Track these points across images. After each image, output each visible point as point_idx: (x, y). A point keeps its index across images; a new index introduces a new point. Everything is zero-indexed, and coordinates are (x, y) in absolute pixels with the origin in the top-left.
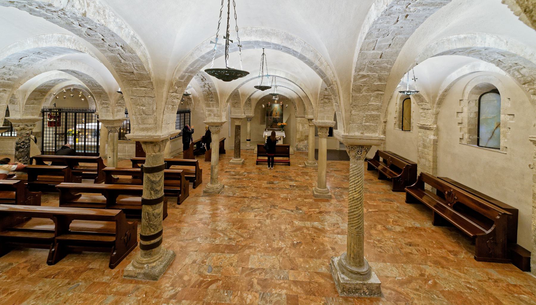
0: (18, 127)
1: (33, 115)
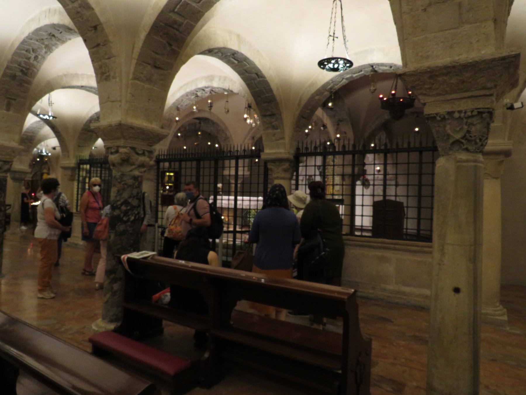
0: (117, 155)
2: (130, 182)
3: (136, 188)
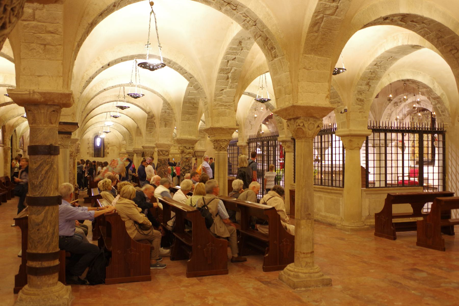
1: (190, 135)
2: (185, 160)
3: (187, 162)
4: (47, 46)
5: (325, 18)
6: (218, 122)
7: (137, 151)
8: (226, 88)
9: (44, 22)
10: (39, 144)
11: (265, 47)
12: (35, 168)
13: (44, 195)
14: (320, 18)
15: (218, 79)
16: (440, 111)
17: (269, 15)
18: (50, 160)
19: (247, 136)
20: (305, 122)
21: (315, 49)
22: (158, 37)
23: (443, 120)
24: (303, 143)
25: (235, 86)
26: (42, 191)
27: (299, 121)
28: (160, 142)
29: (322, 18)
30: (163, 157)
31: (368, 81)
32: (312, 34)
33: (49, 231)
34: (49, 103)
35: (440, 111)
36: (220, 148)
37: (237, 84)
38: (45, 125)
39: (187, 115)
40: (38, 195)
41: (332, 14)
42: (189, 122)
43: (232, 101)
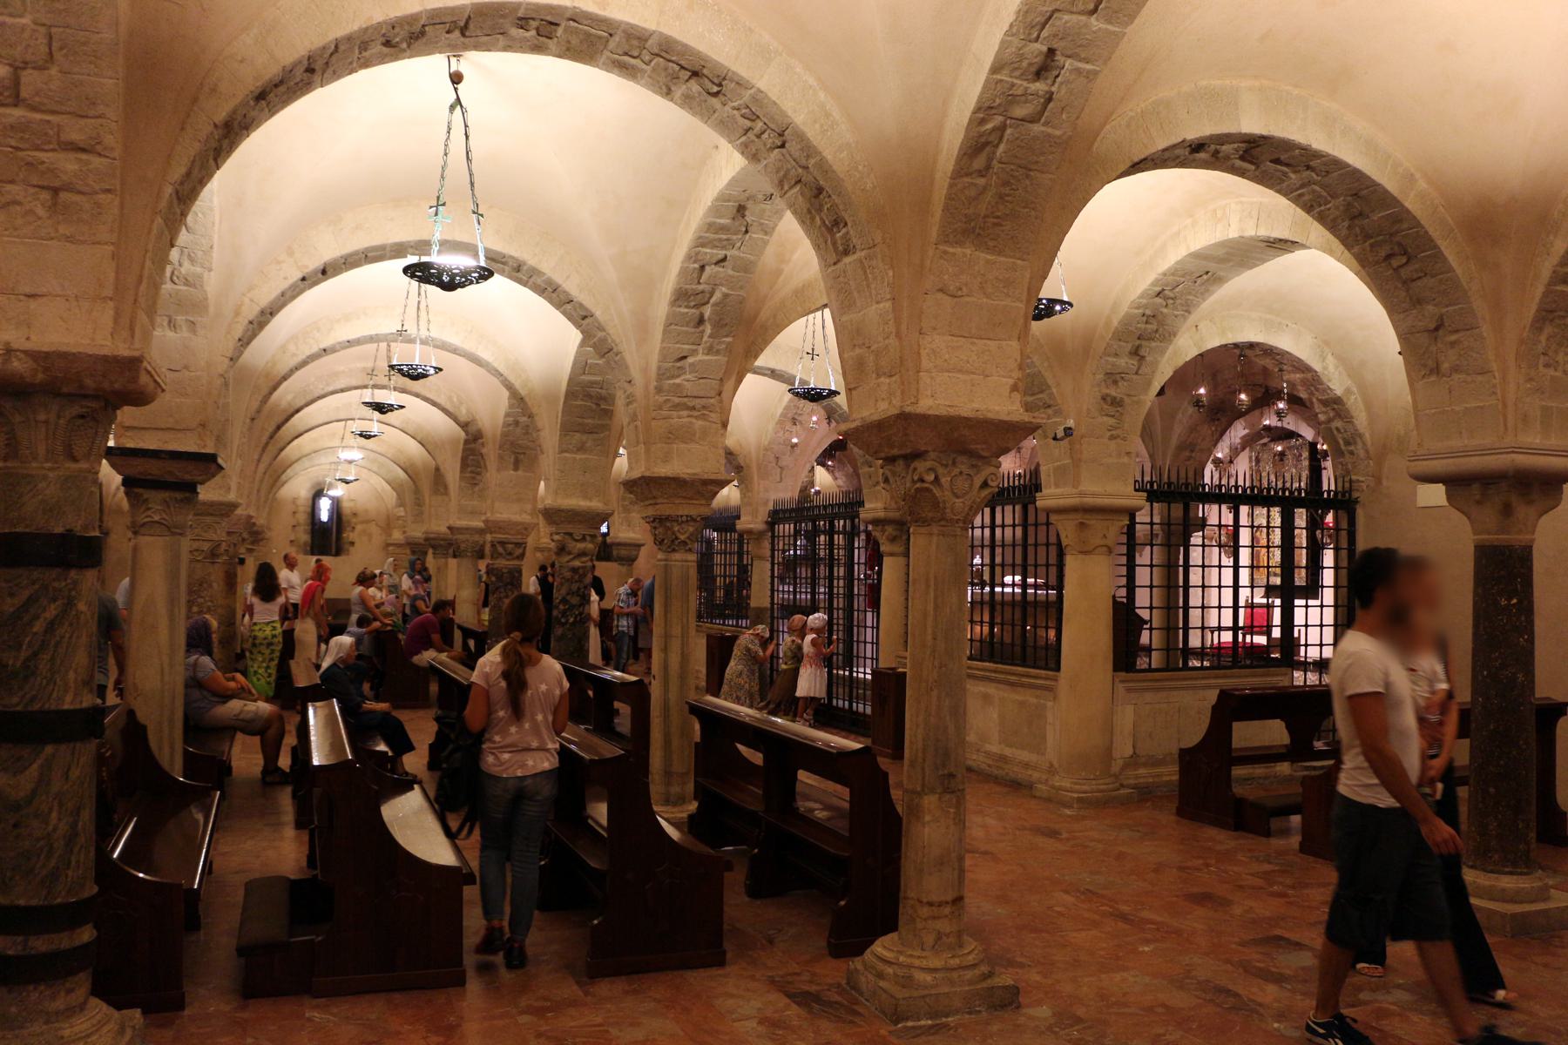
1: (586, 497)
2: (568, 575)
4: (63, 196)
5: (1009, 131)
6: (666, 459)
7: (434, 539)
8: (694, 352)
9: (53, 112)
10: (28, 530)
11: (813, 219)
12: (11, 610)
13: (40, 705)
14: (994, 129)
15: (668, 325)
16: (1341, 442)
17: (828, 115)
18: (64, 584)
19: (766, 503)
20: (941, 470)
21: (977, 231)
22: (472, 184)
23: (1350, 466)
24: (935, 539)
25: (724, 346)
26: (34, 693)
27: (921, 466)
28: (499, 515)
29: (1002, 128)
30: (508, 563)
31: (1138, 342)
32: (967, 180)
33: (55, 830)
34: (65, 390)
35: (1341, 442)
36: (673, 541)
37: (729, 339)
38: (48, 465)
39: (578, 435)
40: (17, 705)
41: (1034, 119)
42: (583, 456)
43: (713, 393)
